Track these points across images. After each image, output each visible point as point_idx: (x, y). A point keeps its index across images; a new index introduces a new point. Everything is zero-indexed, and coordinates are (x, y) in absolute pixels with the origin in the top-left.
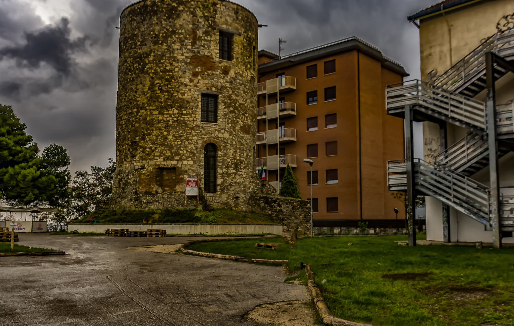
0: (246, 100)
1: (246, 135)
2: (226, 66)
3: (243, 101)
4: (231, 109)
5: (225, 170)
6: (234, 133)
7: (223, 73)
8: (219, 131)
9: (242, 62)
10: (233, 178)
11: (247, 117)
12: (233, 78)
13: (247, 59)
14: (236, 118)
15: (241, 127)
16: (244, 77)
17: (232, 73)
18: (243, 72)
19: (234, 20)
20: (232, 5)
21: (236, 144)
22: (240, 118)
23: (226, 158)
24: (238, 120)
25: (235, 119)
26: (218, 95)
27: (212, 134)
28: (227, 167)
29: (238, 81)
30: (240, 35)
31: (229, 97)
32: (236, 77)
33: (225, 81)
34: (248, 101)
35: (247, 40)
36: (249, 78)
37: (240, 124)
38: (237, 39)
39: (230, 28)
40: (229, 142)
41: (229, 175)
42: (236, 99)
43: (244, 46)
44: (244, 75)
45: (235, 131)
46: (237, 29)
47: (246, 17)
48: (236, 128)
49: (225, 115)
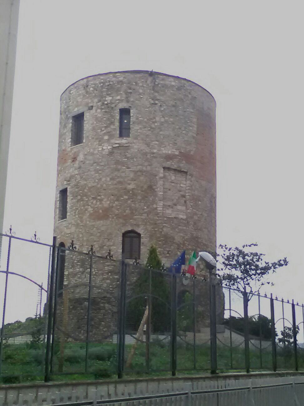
0: (100, 179)
1: (99, 222)
2: (75, 152)
3: (95, 182)
4: (79, 197)
5: (71, 270)
6: (81, 224)
7: (73, 161)
8: (67, 227)
9: (93, 138)
10: (79, 278)
11: (101, 200)
12: (82, 161)
13: (102, 131)
14: (84, 206)
15: (91, 215)
16: (97, 154)
17: (81, 157)
18: (94, 149)
19: (84, 96)
20: (82, 82)
21: (83, 237)
22: (90, 204)
23: (72, 256)
24: (86, 207)
25: (82, 208)
26: (67, 188)
27: (62, 233)
28: (73, 266)
29: (87, 162)
30: (91, 108)
31: (77, 186)
32: (85, 159)
33: (74, 169)
34: (103, 179)
35: (102, 109)
36: (106, 152)
37: (89, 212)
38: (87, 116)
39: (81, 107)
40: (75, 236)
41: (75, 275)
42: (85, 184)
43: (97, 119)
44: (96, 152)
45: (82, 221)
46: (87, 104)
47: (100, 83)
48: (85, 217)
49: (72, 206)
